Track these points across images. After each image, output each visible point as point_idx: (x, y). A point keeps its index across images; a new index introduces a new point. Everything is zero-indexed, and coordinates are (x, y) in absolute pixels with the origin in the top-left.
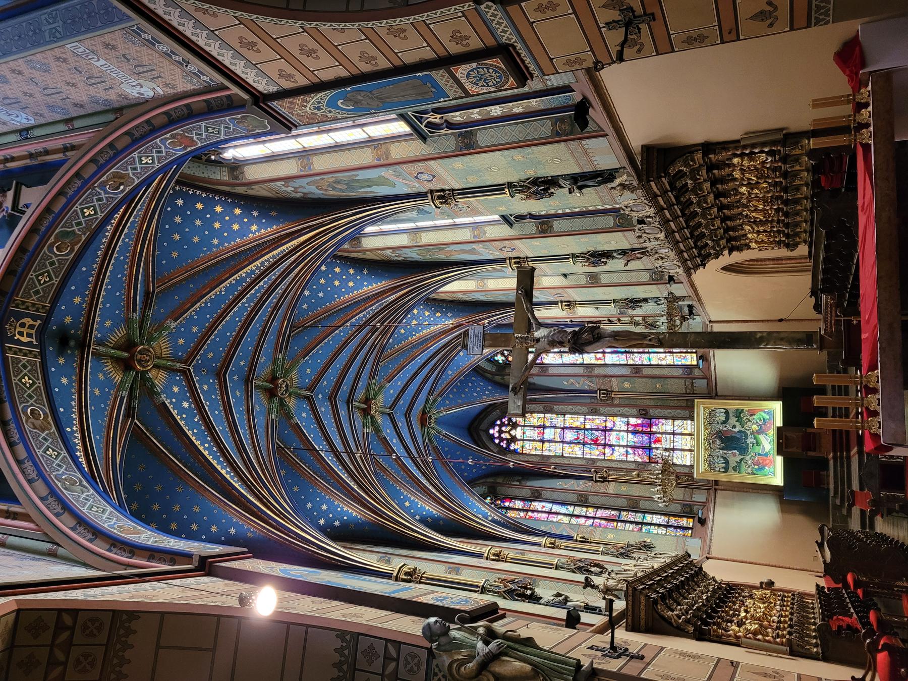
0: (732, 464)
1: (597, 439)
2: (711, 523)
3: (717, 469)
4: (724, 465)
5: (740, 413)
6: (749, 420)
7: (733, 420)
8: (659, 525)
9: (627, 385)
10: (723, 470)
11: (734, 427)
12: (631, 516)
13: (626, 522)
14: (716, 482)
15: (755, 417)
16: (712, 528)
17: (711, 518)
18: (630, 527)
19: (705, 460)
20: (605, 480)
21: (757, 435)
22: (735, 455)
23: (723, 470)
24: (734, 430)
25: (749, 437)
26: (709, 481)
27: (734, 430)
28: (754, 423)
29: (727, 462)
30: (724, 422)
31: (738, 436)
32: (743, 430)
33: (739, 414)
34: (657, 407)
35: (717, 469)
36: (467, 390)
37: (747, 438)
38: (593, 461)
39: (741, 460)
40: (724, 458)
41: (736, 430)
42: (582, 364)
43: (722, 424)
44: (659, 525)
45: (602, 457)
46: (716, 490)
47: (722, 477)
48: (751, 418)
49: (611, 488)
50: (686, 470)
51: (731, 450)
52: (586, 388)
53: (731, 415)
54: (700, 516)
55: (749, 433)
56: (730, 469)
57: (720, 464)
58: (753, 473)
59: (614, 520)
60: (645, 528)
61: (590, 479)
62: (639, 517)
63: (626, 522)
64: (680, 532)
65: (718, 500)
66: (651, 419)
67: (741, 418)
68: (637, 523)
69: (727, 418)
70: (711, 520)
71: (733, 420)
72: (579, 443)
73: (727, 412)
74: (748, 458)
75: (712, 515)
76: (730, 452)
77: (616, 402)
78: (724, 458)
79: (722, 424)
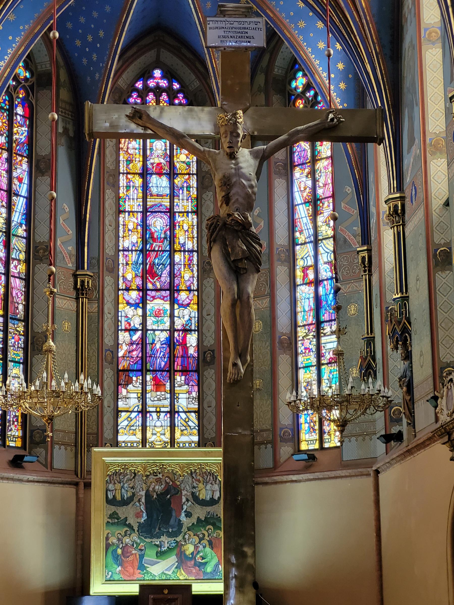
0: (122, 512)
2: (17, 476)
3: (111, 486)
4: (119, 498)
5: (214, 525)
6: (201, 540)
10: (110, 496)
11: (188, 515)
14: (88, 485)
15: (208, 549)
16: (8, 479)
21: (175, 552)
22: (138, 515)
23: (110, 496)
24: (183, 515)
25: (172, 540)
26: (89, 472)
27: (183, 515)
28: (196, 547)
29: (125, 502)
31: (172, 521)
32: (184, 529)
35: (111, 486)
37: (170, 535)
39: (130, 526)
40: (131, 499)
41: (183, 517)
43: (193, 494)
46: (76, 484)
48: (205, 542)
51: (146, 509)
53: (209, 509)
54: (26, 459)
55: (179, 538)
56: (113, 509)
67: (204, 527)
69: (203, 503)
70: (21, 477)
75: (31, 478)
76: (143, 508)
79: (193, 494)
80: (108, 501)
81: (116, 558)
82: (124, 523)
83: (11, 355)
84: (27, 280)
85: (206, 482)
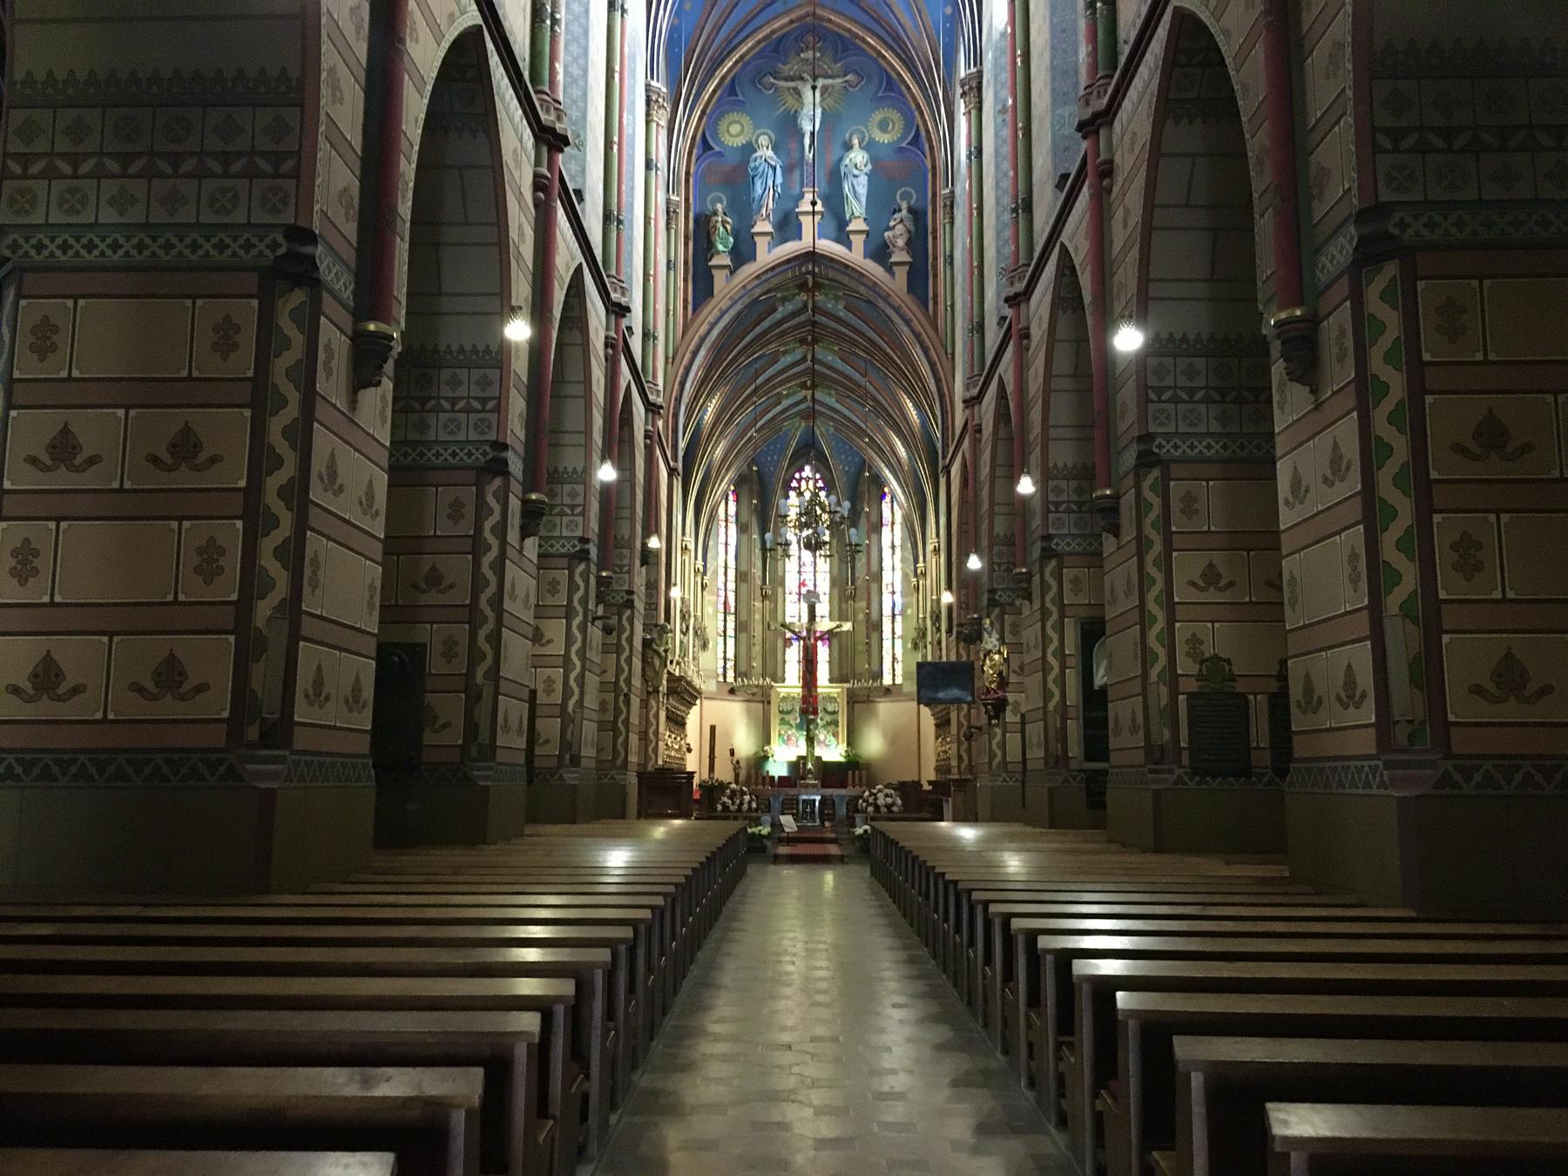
0: (787, 717)
1: (804, 585)
7: (828, 718)
8: (725, 652)
9: (861, 617)
11: (822, 719)
12: (731, 625)
13: (725, 621)
14: (769, 703)
15: (832, 738)
17: (736, 699)
18: (721, 624)
19: (789, 694)
20: (764, 597)
29: (788, 713)
30: (825, 710)
33: (836, 723)
34: (840, 646)
36: (850, 458)
38: (783, 584)
40: (792, 711)
41: (819, 721)
42: (881, 569)
44: (725, 652)
45: (787, 591)
46: (763, 702)
47: (774, 709)
49: (758, 604)
50: (780, 674)
52: (857, 575)
53: (834, 717)
56: (782, 716)
57: (785, 707)
58: (780, 735)
59: (725, 609)
60: (721, 640)
61: (764, 582)
62: (731, 632)
63: (725, 621)
64: (720, 671)
65: (753, 705)
66: (828, 639)
68: (725, 632)
71: (828, 718)
72: (800, 566)
73: (834, 713)
74: (794, 731)
77: (844, 606)
78: (792, 711)
80: (780, 712)
81: (784, 741)
82: (788, 723)
83: (728, 634)
84: (736, 592)
85: (831, 702)
